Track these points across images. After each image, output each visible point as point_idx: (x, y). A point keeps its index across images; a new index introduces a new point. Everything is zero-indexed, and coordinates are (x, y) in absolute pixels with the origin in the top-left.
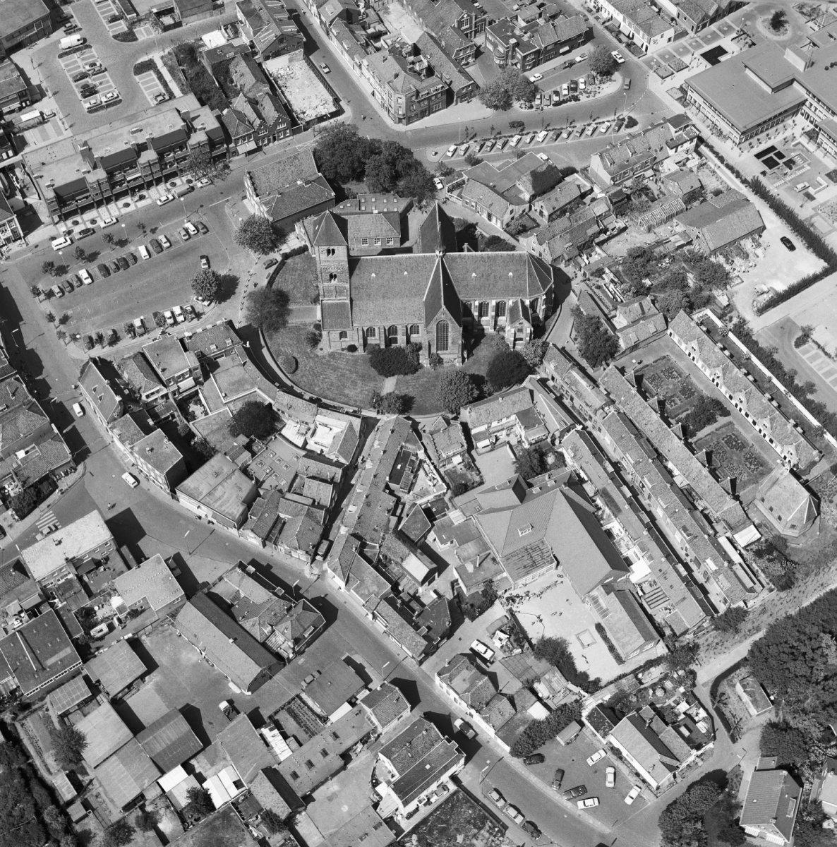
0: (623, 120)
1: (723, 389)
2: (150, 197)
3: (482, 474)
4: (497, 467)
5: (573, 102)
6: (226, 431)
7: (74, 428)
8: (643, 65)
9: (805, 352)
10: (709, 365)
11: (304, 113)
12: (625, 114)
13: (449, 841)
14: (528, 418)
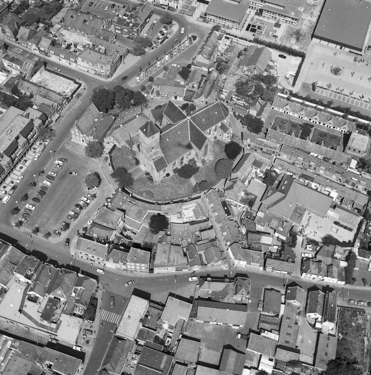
1: (305, 118)
2: (29, 159)
3: (253, 193)
4: (257, 188)
5: (167, 40)
6: (150, 234)
7: (82, 270)
8: (180, 14)
9: (318, 92)
10: (296, 112)
11: (65, 92)
12: (190, 36)
13: (351, 327)
14: (257, 164)
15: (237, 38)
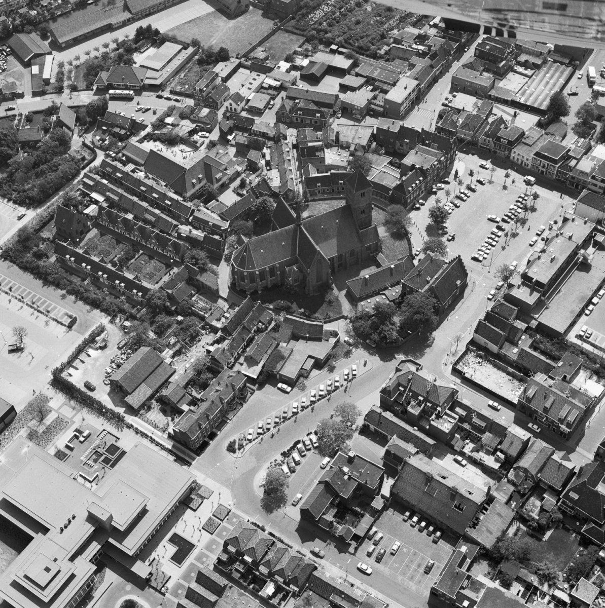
0: (239, 449)
15: (151, 438)
